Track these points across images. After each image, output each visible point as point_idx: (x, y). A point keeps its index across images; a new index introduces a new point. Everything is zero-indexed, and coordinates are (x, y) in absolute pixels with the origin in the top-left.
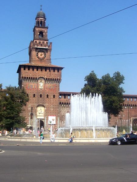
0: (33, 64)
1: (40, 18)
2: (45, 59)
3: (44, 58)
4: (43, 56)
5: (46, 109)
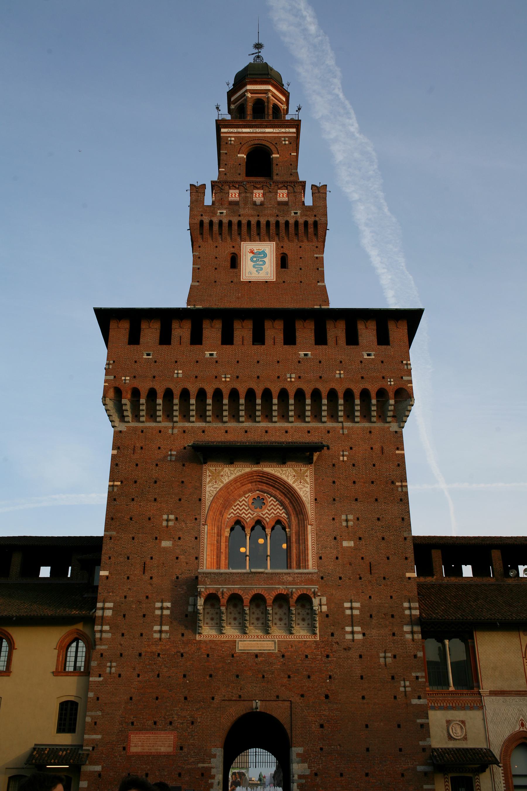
1: (249, 87)
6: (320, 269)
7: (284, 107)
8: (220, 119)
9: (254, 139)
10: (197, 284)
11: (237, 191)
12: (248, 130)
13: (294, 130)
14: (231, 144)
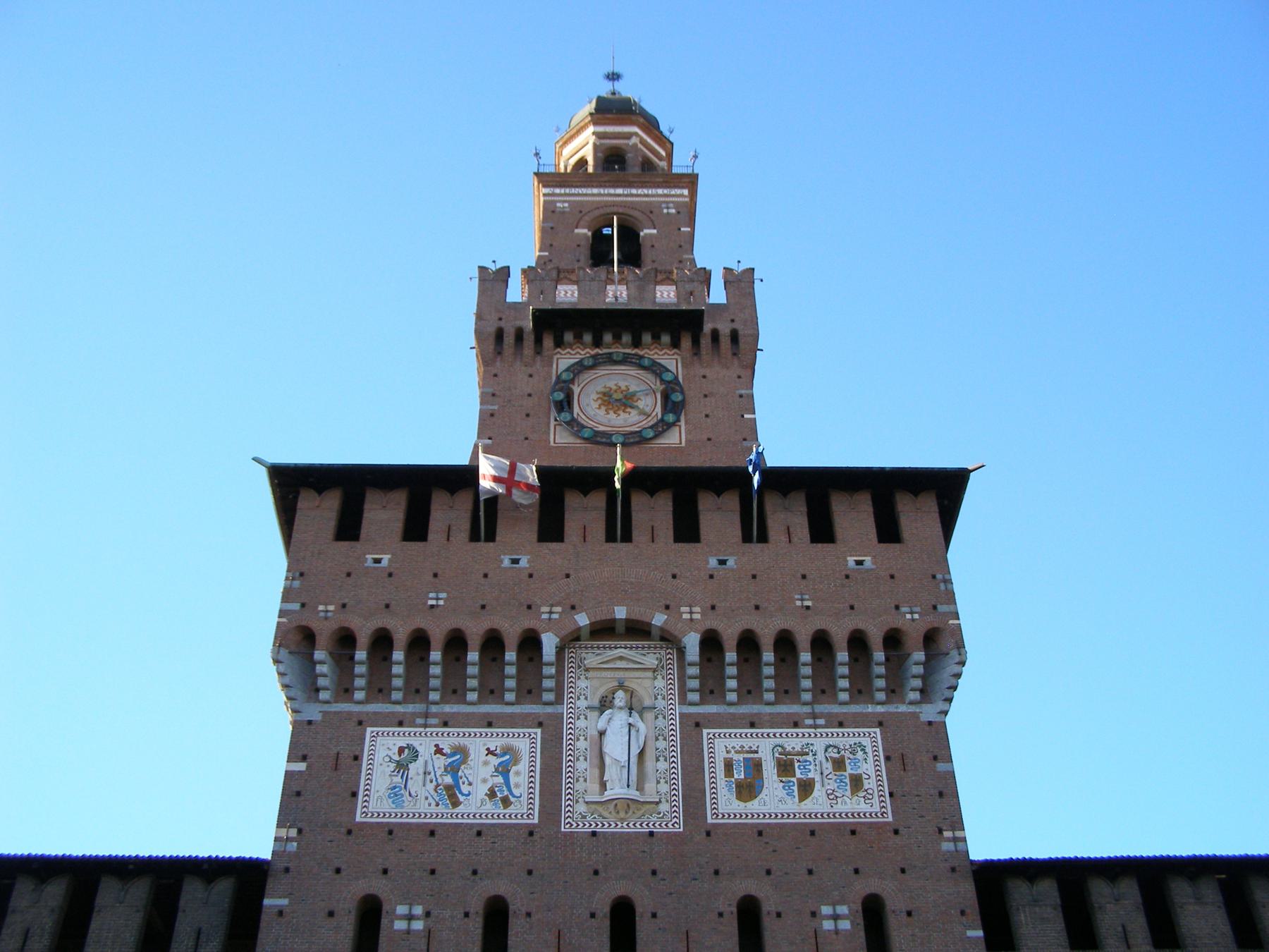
2: (674, 438)
3: (662, 427)
6: (746, 416)
7: (663, 164)
8: (541, 170)
9: (607, 204)
10: (490, 441)
11: (576, 287)
12: (595, 191)
13: (686, 192)
14: (563, 213)
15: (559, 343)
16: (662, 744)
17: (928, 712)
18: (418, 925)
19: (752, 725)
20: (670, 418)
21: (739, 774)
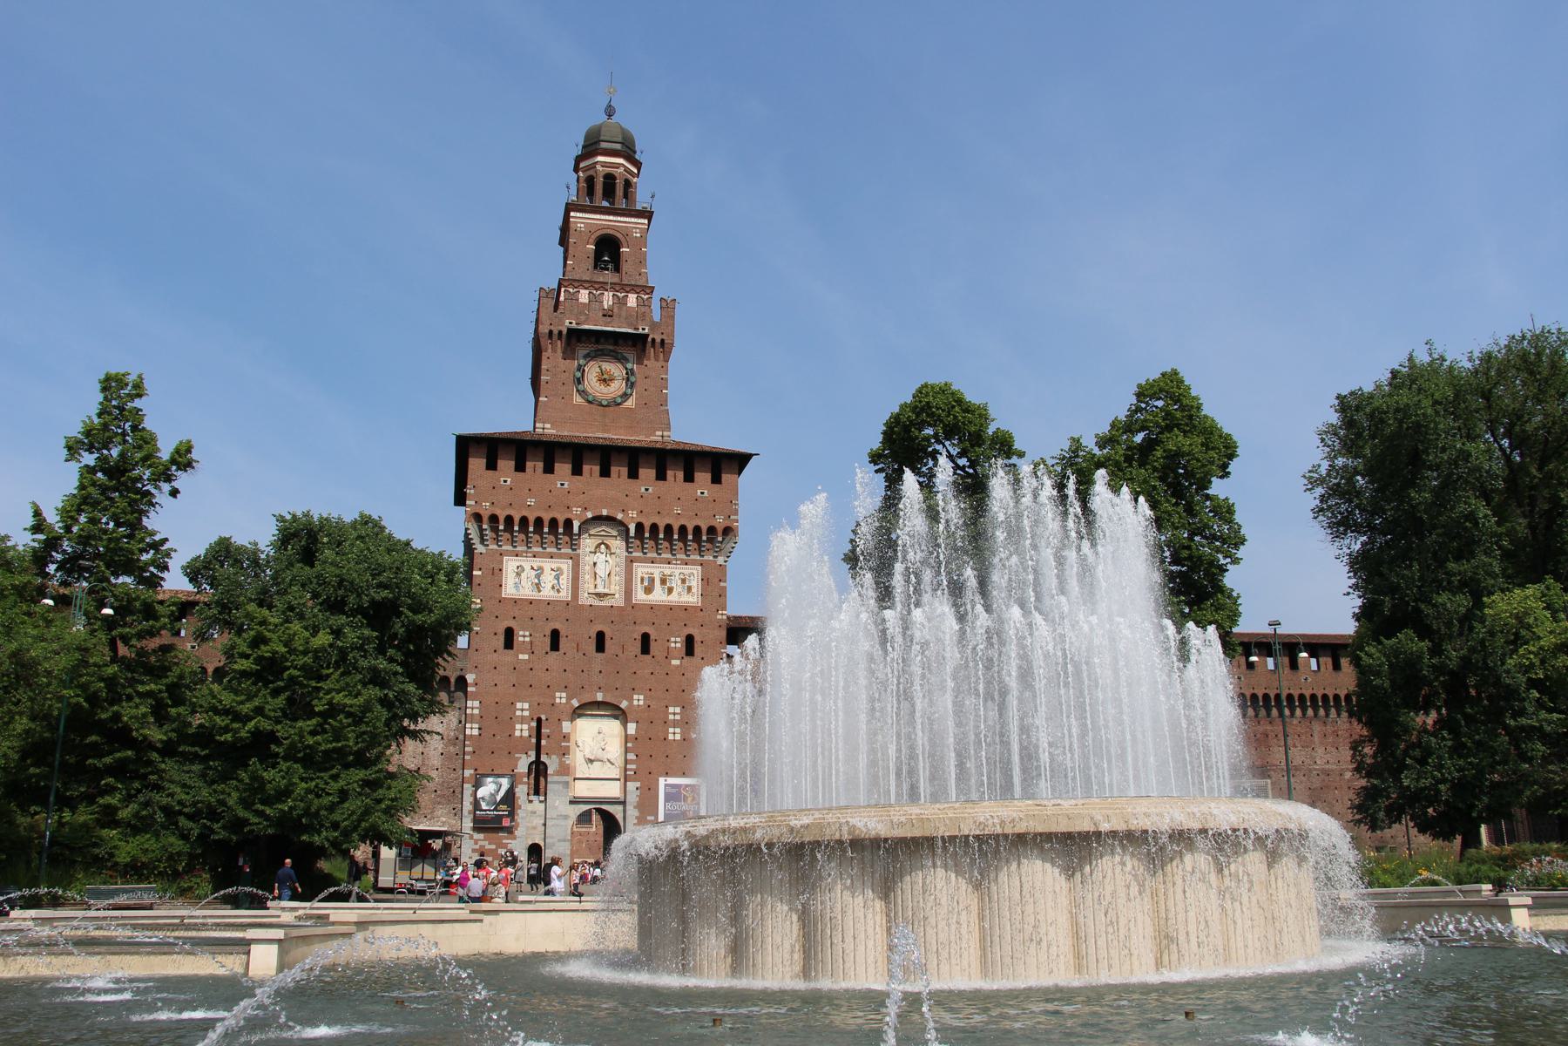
0: (548, 430)
1: (600, 158)
2: (630, 403)
3: (625, 396)
4: (617, 387)
5: (634, 732)
12: (598, 216)
13: (646, 221)
14: (581, 232)
15: (579, 341)
16: (618, 569)
17: (720, 560)
18: (527, 639)
19: (653, 562)
20: (629, 391)
21: (646, 583)
